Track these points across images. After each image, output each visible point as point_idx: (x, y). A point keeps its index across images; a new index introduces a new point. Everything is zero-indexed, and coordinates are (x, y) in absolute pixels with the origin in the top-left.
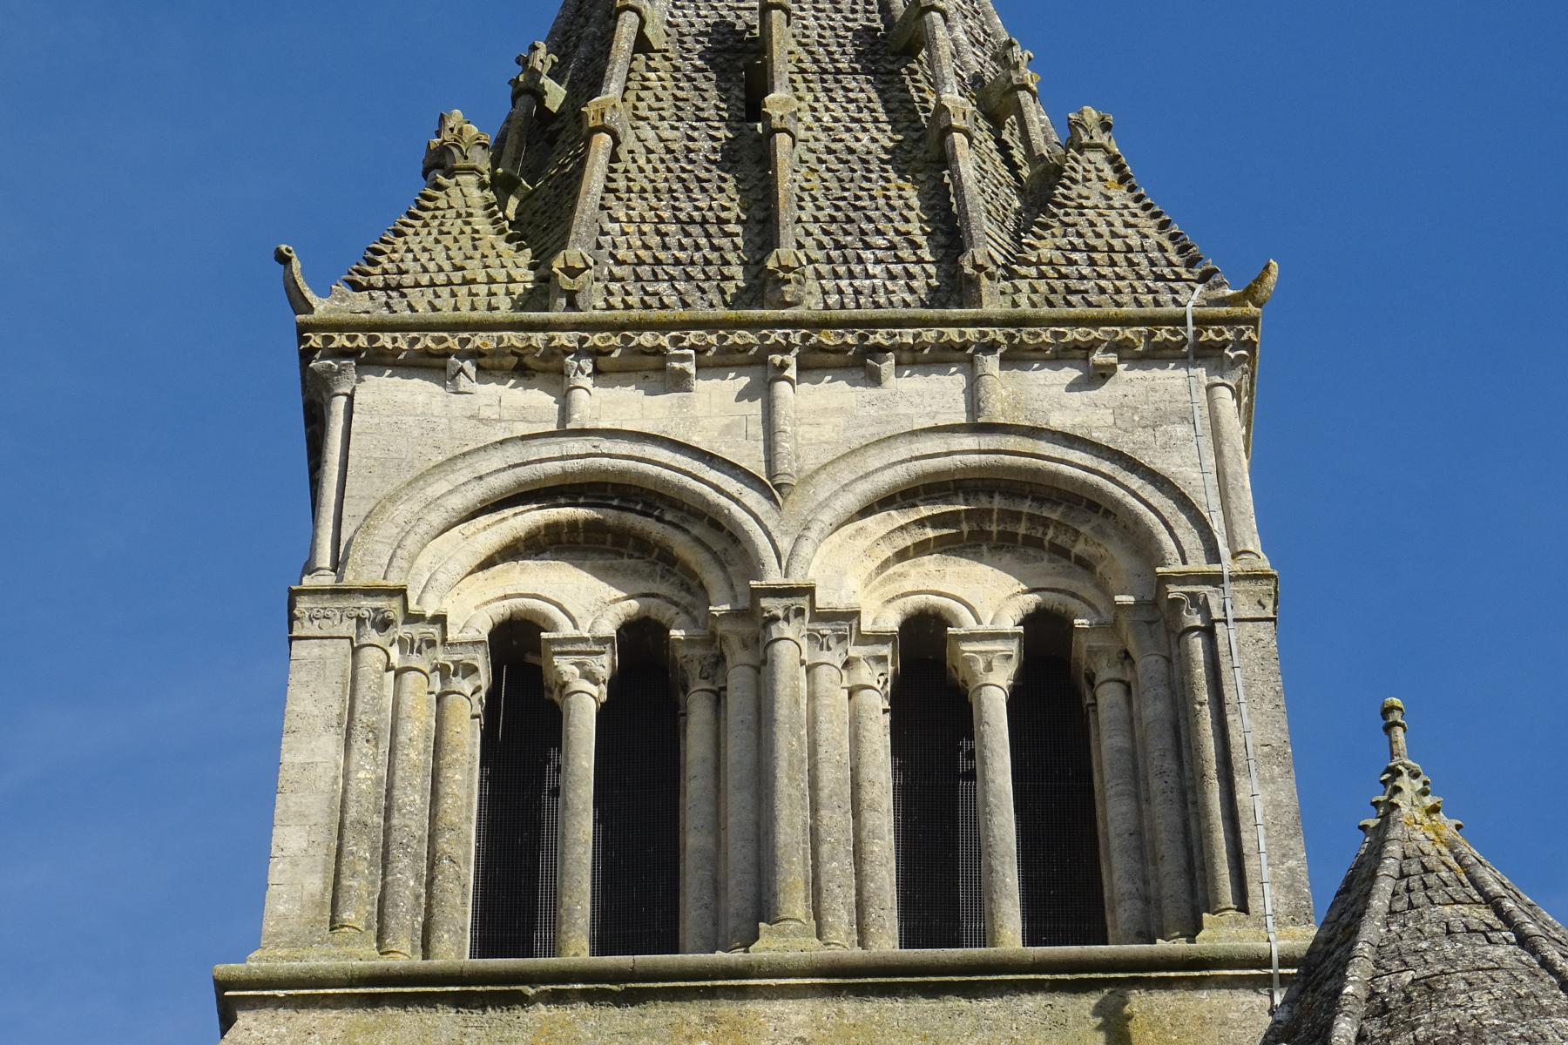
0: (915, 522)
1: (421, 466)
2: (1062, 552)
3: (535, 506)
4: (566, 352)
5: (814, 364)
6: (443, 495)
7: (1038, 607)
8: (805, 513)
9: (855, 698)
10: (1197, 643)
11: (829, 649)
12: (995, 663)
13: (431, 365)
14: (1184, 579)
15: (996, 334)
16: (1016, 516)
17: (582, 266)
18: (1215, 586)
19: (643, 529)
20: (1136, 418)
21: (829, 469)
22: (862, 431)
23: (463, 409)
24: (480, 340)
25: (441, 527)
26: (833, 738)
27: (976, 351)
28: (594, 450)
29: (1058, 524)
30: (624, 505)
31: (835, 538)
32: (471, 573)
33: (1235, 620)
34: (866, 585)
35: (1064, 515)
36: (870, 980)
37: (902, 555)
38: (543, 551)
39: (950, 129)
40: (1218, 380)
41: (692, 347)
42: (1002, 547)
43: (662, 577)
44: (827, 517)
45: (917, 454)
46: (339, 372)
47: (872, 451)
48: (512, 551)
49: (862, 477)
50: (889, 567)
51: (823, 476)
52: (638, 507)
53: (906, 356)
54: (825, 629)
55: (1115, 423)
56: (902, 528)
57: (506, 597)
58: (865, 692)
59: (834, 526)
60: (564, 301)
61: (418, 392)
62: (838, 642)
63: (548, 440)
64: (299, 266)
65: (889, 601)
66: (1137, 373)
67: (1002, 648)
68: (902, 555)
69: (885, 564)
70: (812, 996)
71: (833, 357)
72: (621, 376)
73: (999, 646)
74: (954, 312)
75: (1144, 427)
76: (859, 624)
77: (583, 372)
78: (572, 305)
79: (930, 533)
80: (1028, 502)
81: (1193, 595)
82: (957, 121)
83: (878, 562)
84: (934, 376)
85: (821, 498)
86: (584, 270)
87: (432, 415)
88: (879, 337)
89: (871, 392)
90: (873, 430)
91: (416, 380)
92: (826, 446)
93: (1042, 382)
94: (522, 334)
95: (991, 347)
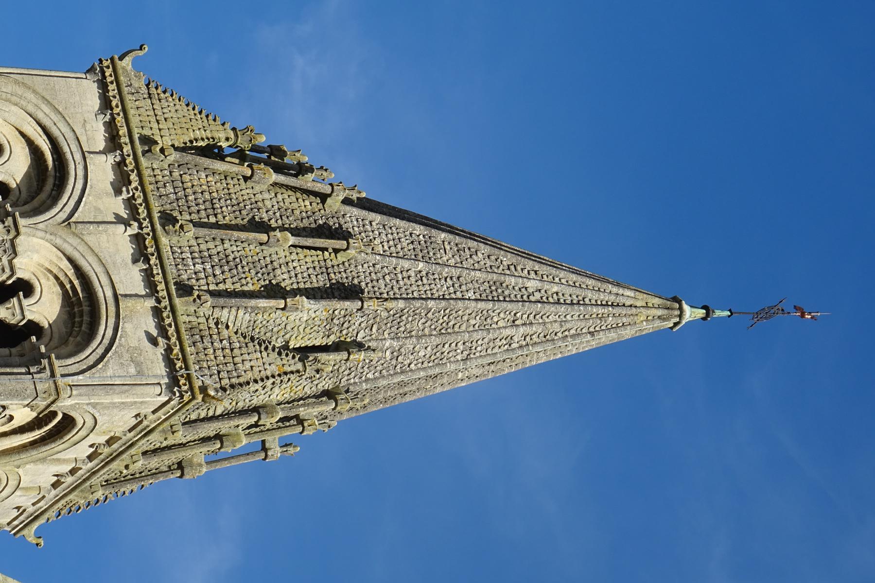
0: (70, 279)
1: (55, 103)
2: (70, 334)
3: (50, 147)
4: (122, 151)
5: (138, 239)
6: (42, 111)
7: (43, 327)
8: (59, 234)
10: (23, 370)
13: (106, 104)
14: (51, 365)
15: (165, 303)
16: (81, 316)
17: (166, 154)
18: (51, 376)
20: (135, 355)
21: (83, 243)
22: (107, 257)
23: (88, 118)
24: (120, 120)
25: (28, 112)
27: (156, 297)
28: (77, 163)
29: (80, 330)
30: (57, 178)
31: (55, 249)
32: (17, 129)
33: (34, 382)
34: (39, 265)
35: (85, 332)
37: (57, 278)
38: (34, 155)
39: (285, 299)
40: (164, 387)
41: (134, 194)
42: (70, 315)
43: (30, 195)
44: (59, 241)
45: (98, 275)
46: (95, 73)
47: (96, 258)
48: (30, 143)
49: (82, 255)
51: (79, 241)
52: (57, 182)
53: (149, 272)
54: (8, 245)
55: (131, 347)
56: (66, 275)
57: (9, 142)
59: (56, 246)
60: (147, 148)
61: (95, 103)
63: (79, 146)
64: (140, 54)
65: (34, 274)
66: (161, 358)
68: (57, 278)
69: (51, 272)
71: (142, 246)
72: (119, 173)
73: (18, 311)
74: (173, 288)
75: (131, 358)
76: (14, 258)
77: (115, 157)
78: (144, 153)
79: (68, 286)
80: (89, 319)
81: (45, 368)
82: (290, 301)
83: (49, 268)
84: (143, 284)
85: (68, 239)
86: (164, 155)
87: (82, 107)
88: (153, 260)
89: (129, 261)
90: (109, 260)
91: (99, 101)
92: (97, 244)
93: (147, 322)
94: (127, 134)
95: (159, 301)
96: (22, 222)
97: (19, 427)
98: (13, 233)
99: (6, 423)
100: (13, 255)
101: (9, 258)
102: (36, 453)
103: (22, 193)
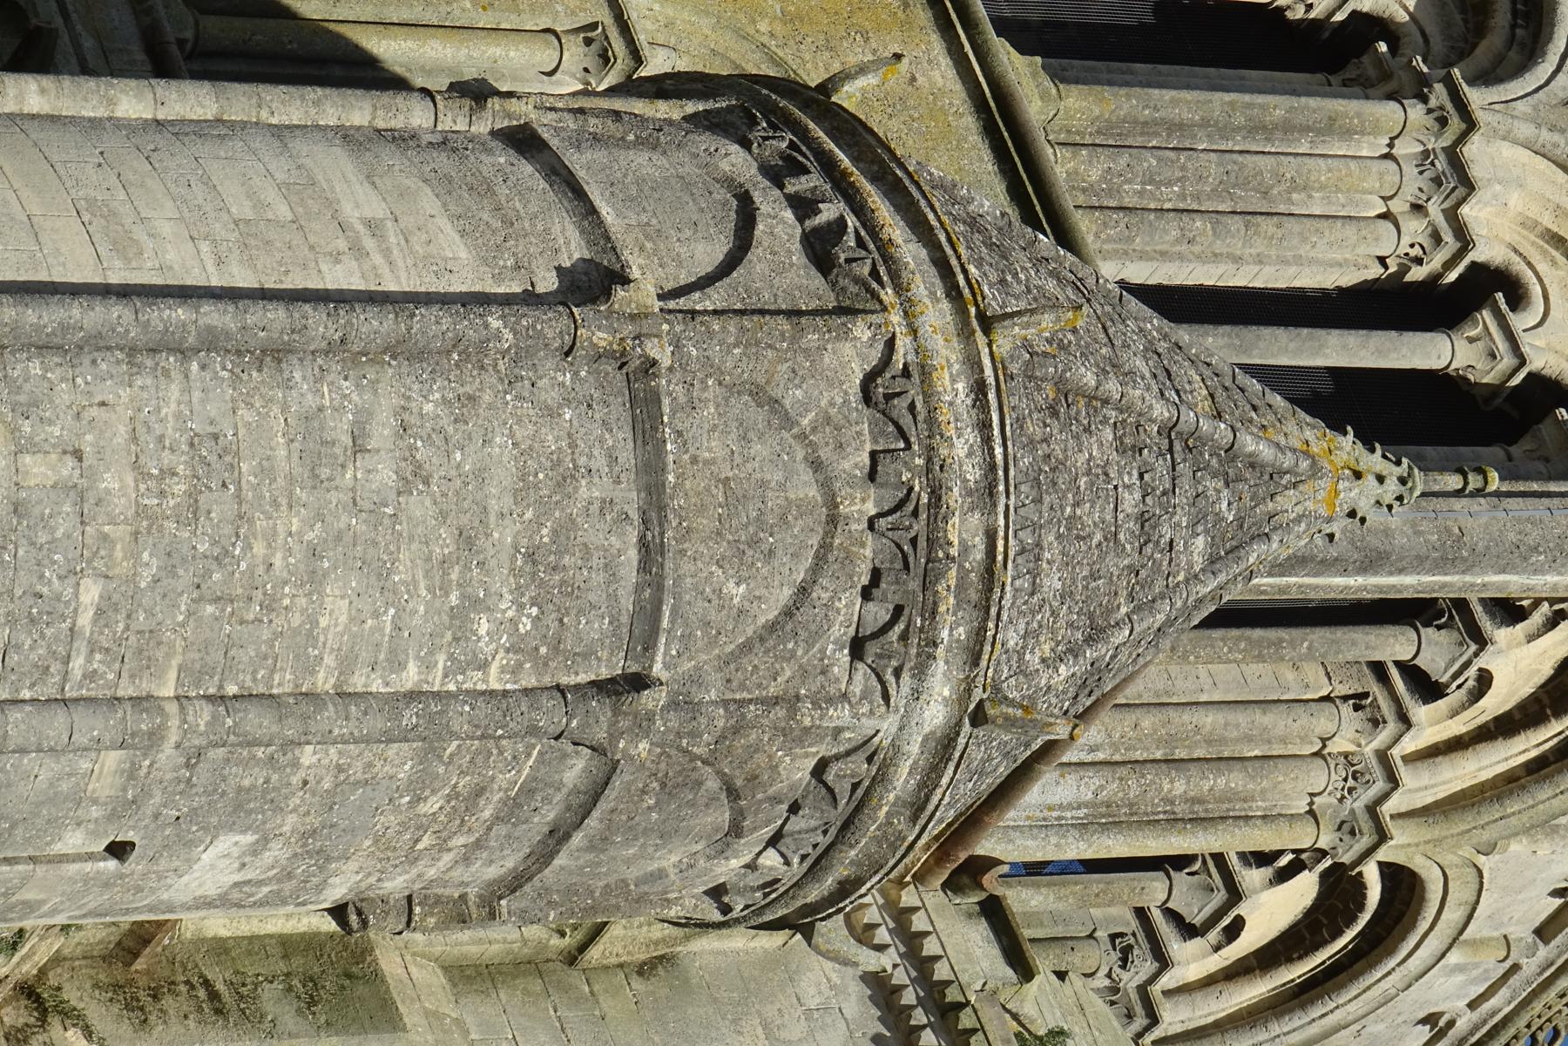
9: (1381, 222)
11: (1421, 173)
12: (1480, 344)
19: (1495, 11)
26: (1309, 171)
36: (1006, 134)
50: (1557, 249)
54: (1441, 164)
58: (1391, 226)
62: (1431, 179)
65: (1516, 251)
67: (1500, 347)
70: (967, 90)
73: (1502, 345)
76: (1463, 200)
83: (1555, 229)
96: (1476, 97)
97: (1496, 719)
98: (1456, 124)
99: (1464, 707)
100: (1461, 191)
101: (1446, 205)
102: (1550, 793)
103: (1431, 40)
